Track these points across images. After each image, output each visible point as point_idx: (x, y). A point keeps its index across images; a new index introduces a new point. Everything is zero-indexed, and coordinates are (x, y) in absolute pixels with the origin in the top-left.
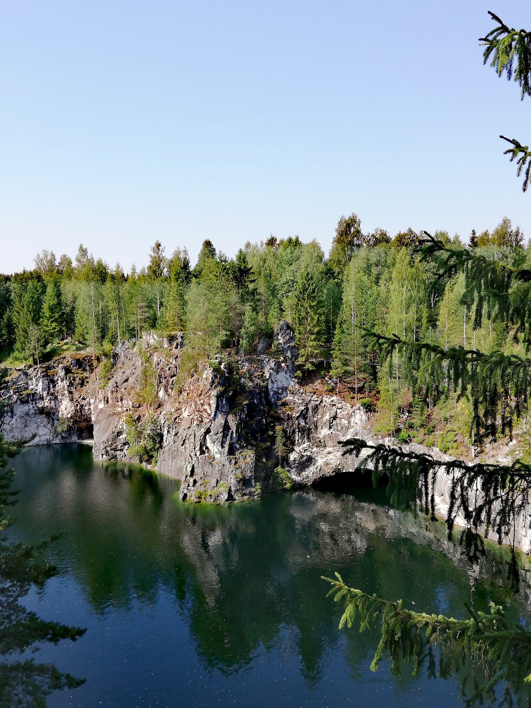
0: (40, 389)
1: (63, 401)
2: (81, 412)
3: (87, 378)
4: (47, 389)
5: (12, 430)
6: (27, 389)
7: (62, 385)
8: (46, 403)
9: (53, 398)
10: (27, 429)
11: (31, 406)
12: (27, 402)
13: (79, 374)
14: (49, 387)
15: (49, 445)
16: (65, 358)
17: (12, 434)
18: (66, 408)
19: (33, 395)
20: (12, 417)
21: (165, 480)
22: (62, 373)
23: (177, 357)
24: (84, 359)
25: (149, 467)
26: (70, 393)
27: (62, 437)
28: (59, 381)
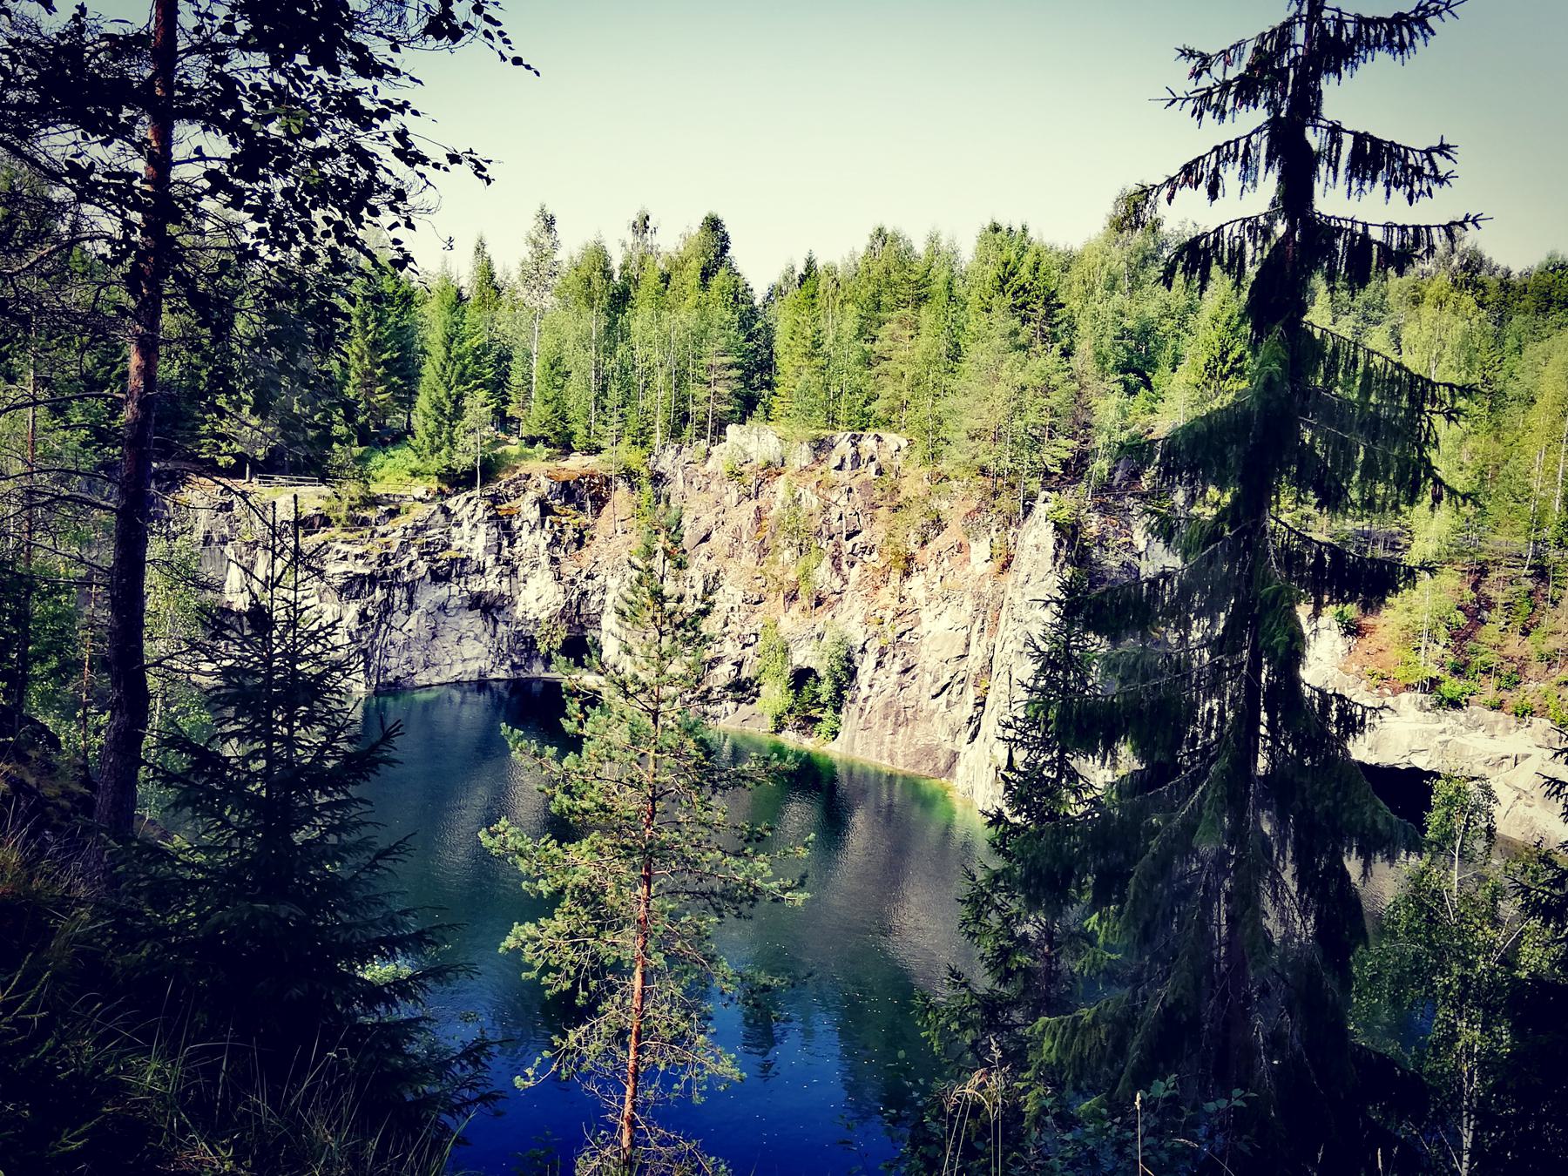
0: (481, 550)
1: (529, 580)
2: (578, 607)
3: (587, 527)
4: (495, 549)
5: (407, 646)
6: (447, 546)
7: (533, 541)
8: (490, 584)
9: (507, 570)
10: (437, 642)
11: (455, 590)
12: (446, 578)
13: (572, 520)
14: (500, 545)
15: (482, 684)
16: (529, 476)
17: (406, 654)
18: (538, 598)
19: (464, 561)
20: (408, 613)
21: (866, 775)
22: (534, 514)
23: (850, 490)
24: (577, 482)
25: (809, 744)
26: (554, 560)
27: (514, 666)
28: (524, 533)
